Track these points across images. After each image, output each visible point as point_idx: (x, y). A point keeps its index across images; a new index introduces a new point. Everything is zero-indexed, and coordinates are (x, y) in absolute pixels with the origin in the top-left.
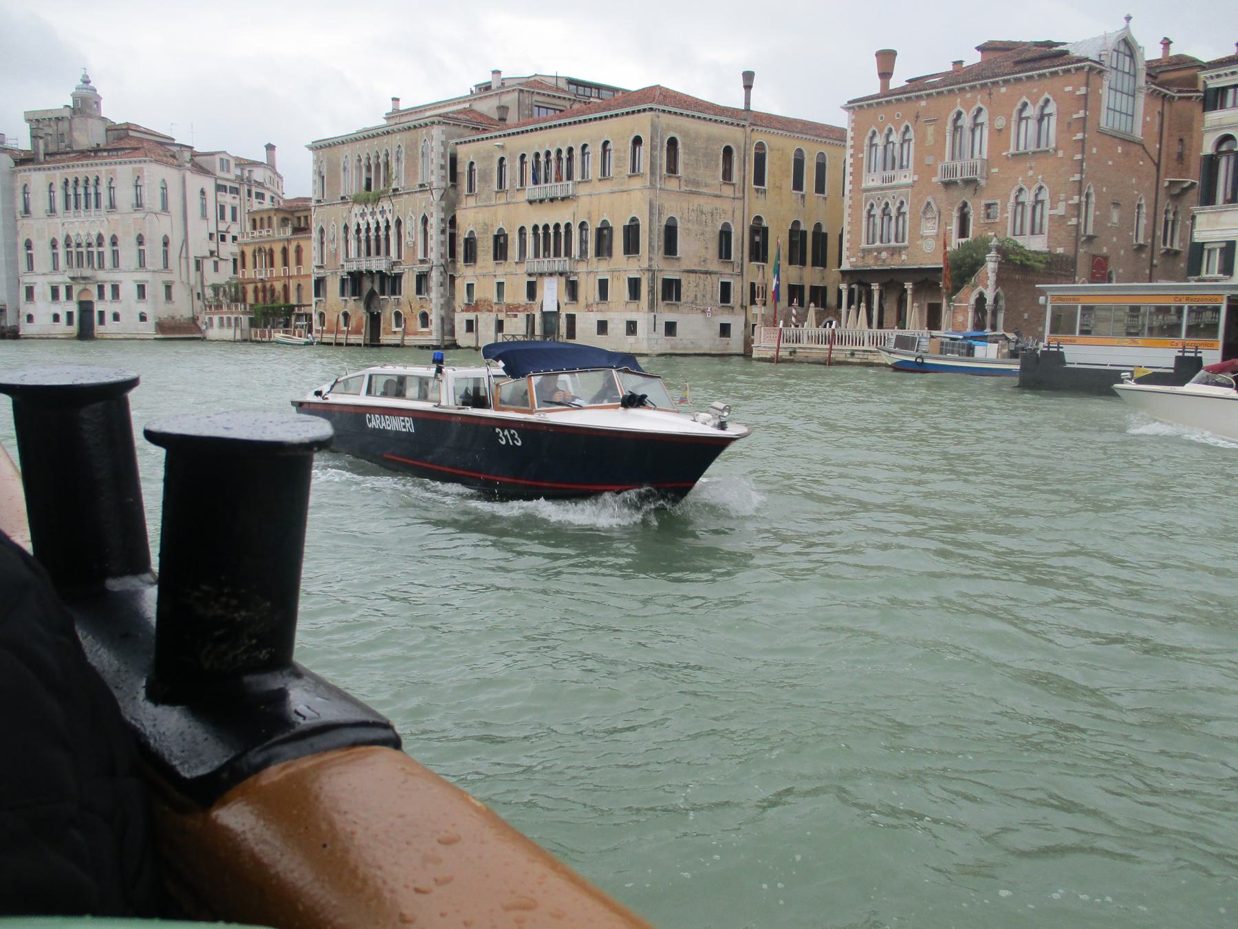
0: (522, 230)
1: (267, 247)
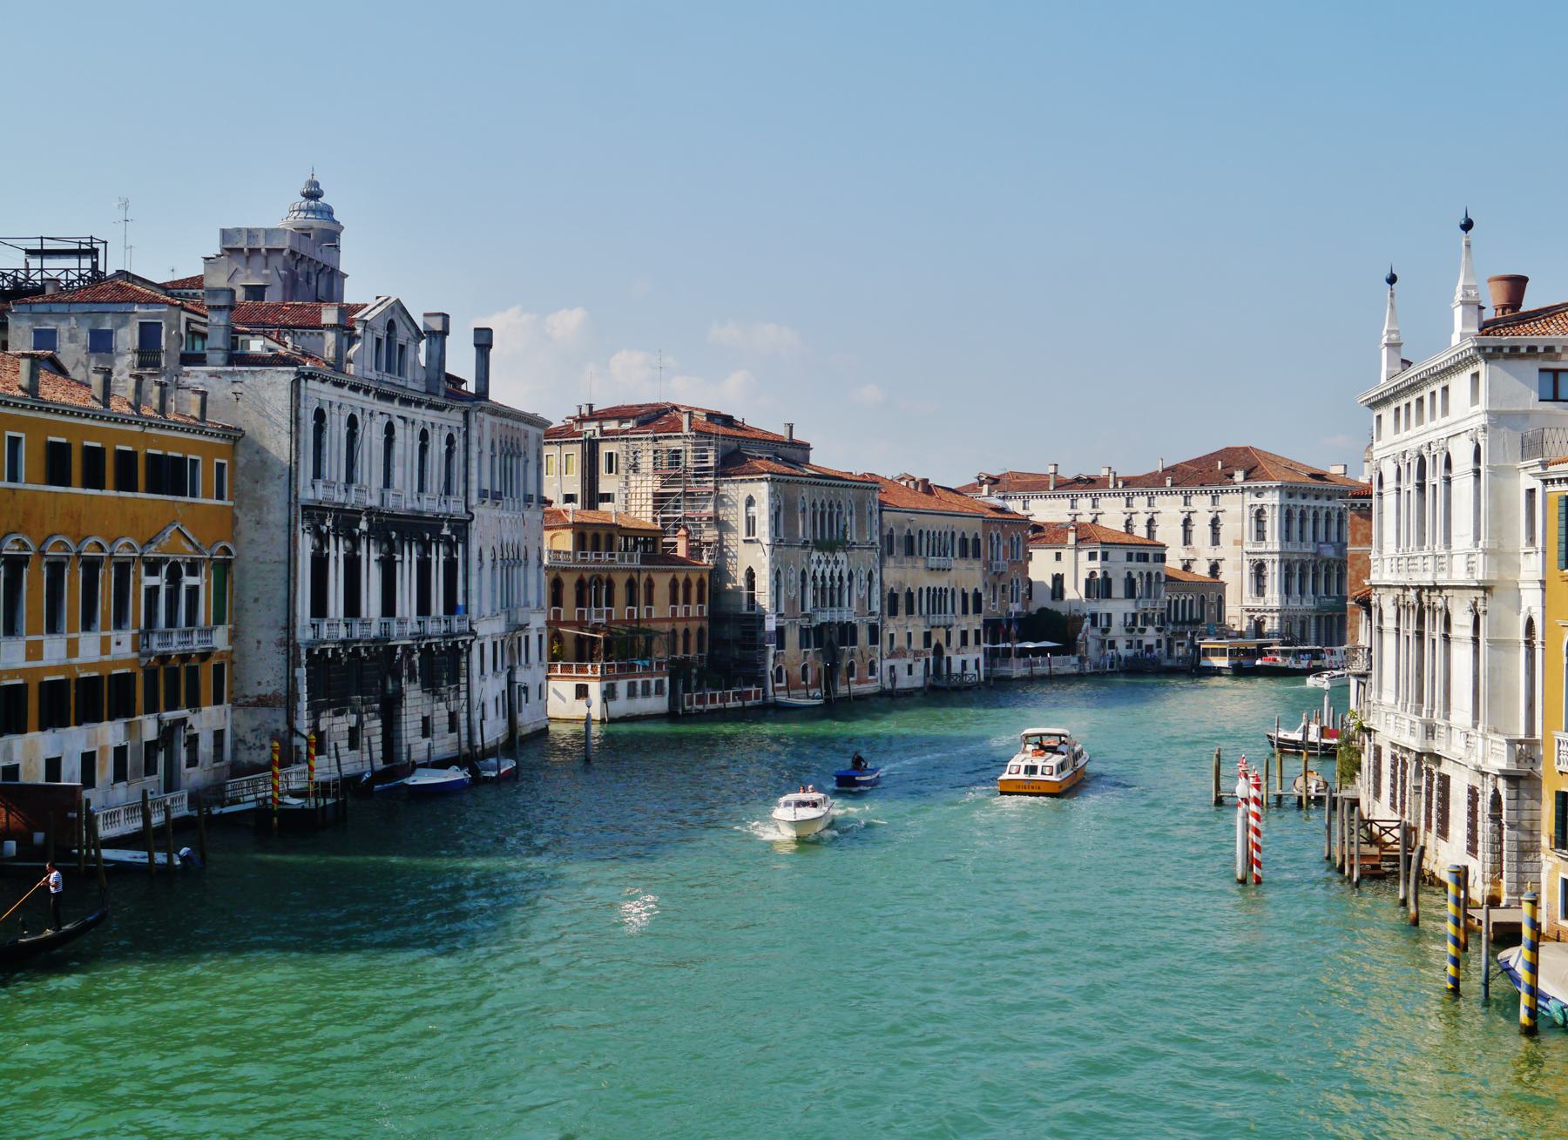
1: (605, 576)
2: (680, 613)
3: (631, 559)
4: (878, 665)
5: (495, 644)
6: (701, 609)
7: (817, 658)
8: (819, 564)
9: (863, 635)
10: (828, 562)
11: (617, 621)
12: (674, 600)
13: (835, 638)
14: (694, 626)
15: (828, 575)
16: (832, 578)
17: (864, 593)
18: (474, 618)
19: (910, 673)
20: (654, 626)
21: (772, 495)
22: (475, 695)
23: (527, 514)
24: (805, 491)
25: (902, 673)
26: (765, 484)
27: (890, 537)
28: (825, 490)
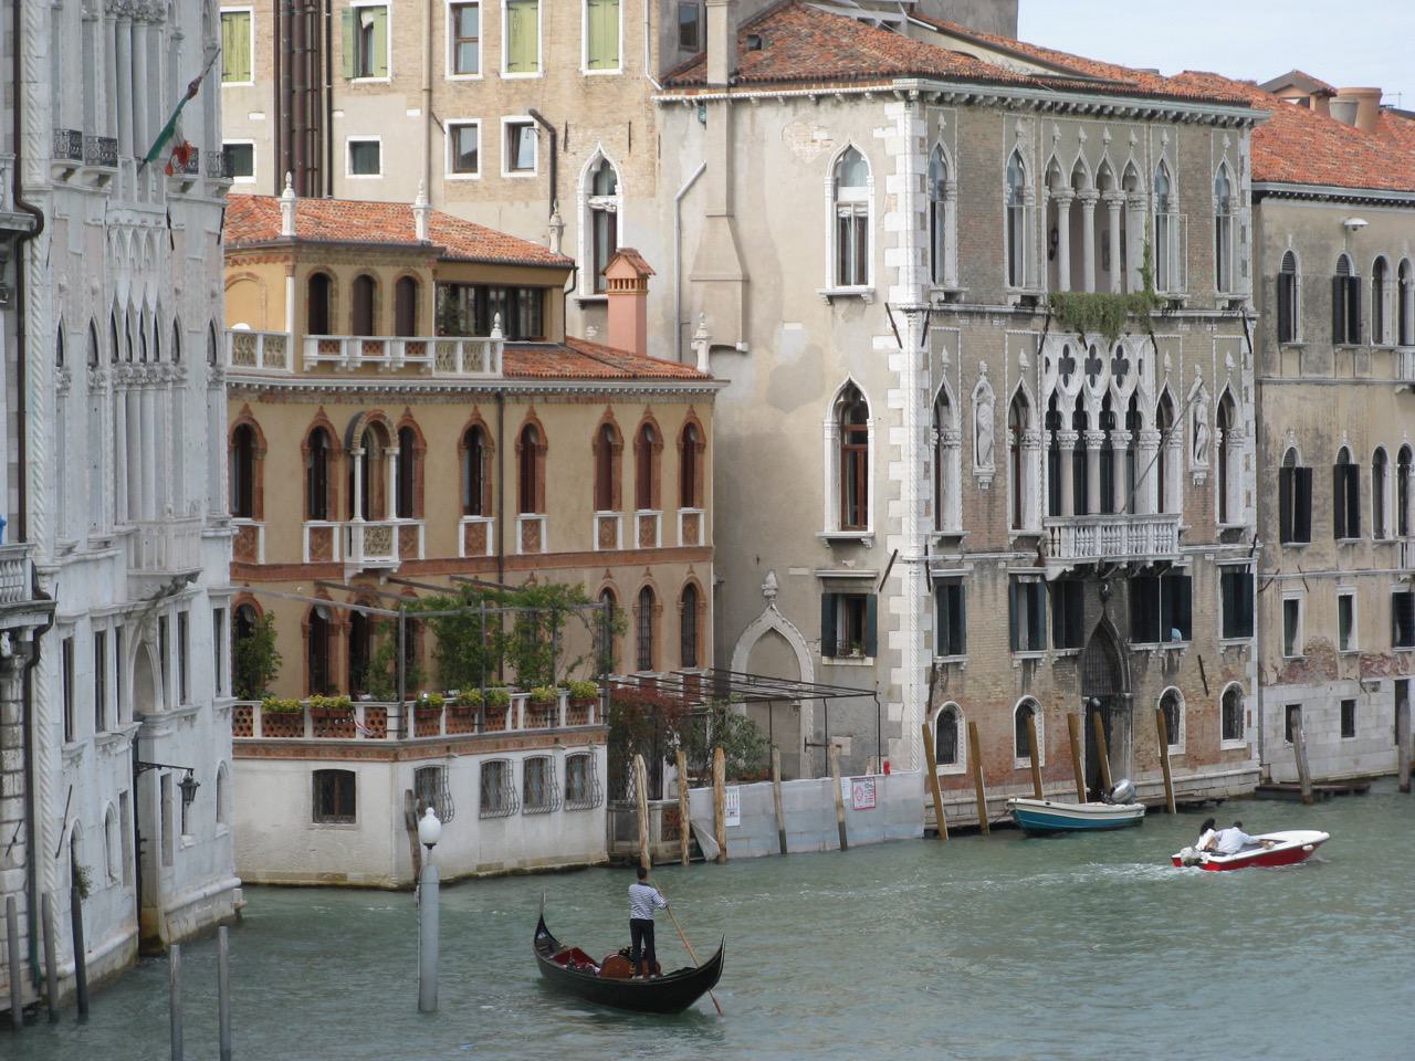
0: (1380, 454)
2: (628, 536)
3: (474, 363)
4: (1249, 703)
5: (100, 638)
6: (691, 520)
7: (1064, 684)
8: (1060, 371)
9: (1208, 603)
10: (1093, 367)
11: (435, 565)
12: (607, 495)
13: (1119, 614)
14: (669, 581)
15: (1094, 410)
16: (1107, 421)
17: (1204, 465)
18: (44, 557)
19: (1348, 729)
20: (546, 577)
21: (930, 147)
22: (49, 810)
23: (180, 214)
24: (1025, 133)
25: (1322, 730)
26: (896, 110)
27: (1285, 282)
28: (1083, 129)
